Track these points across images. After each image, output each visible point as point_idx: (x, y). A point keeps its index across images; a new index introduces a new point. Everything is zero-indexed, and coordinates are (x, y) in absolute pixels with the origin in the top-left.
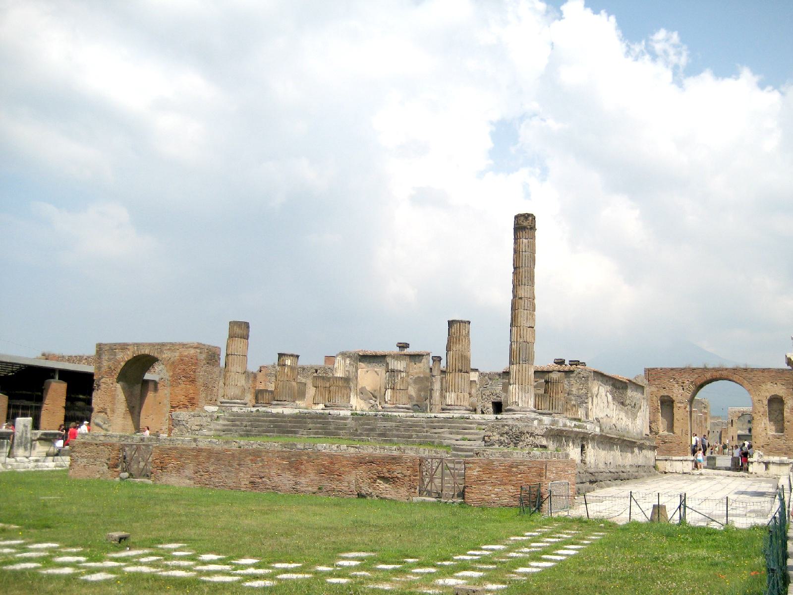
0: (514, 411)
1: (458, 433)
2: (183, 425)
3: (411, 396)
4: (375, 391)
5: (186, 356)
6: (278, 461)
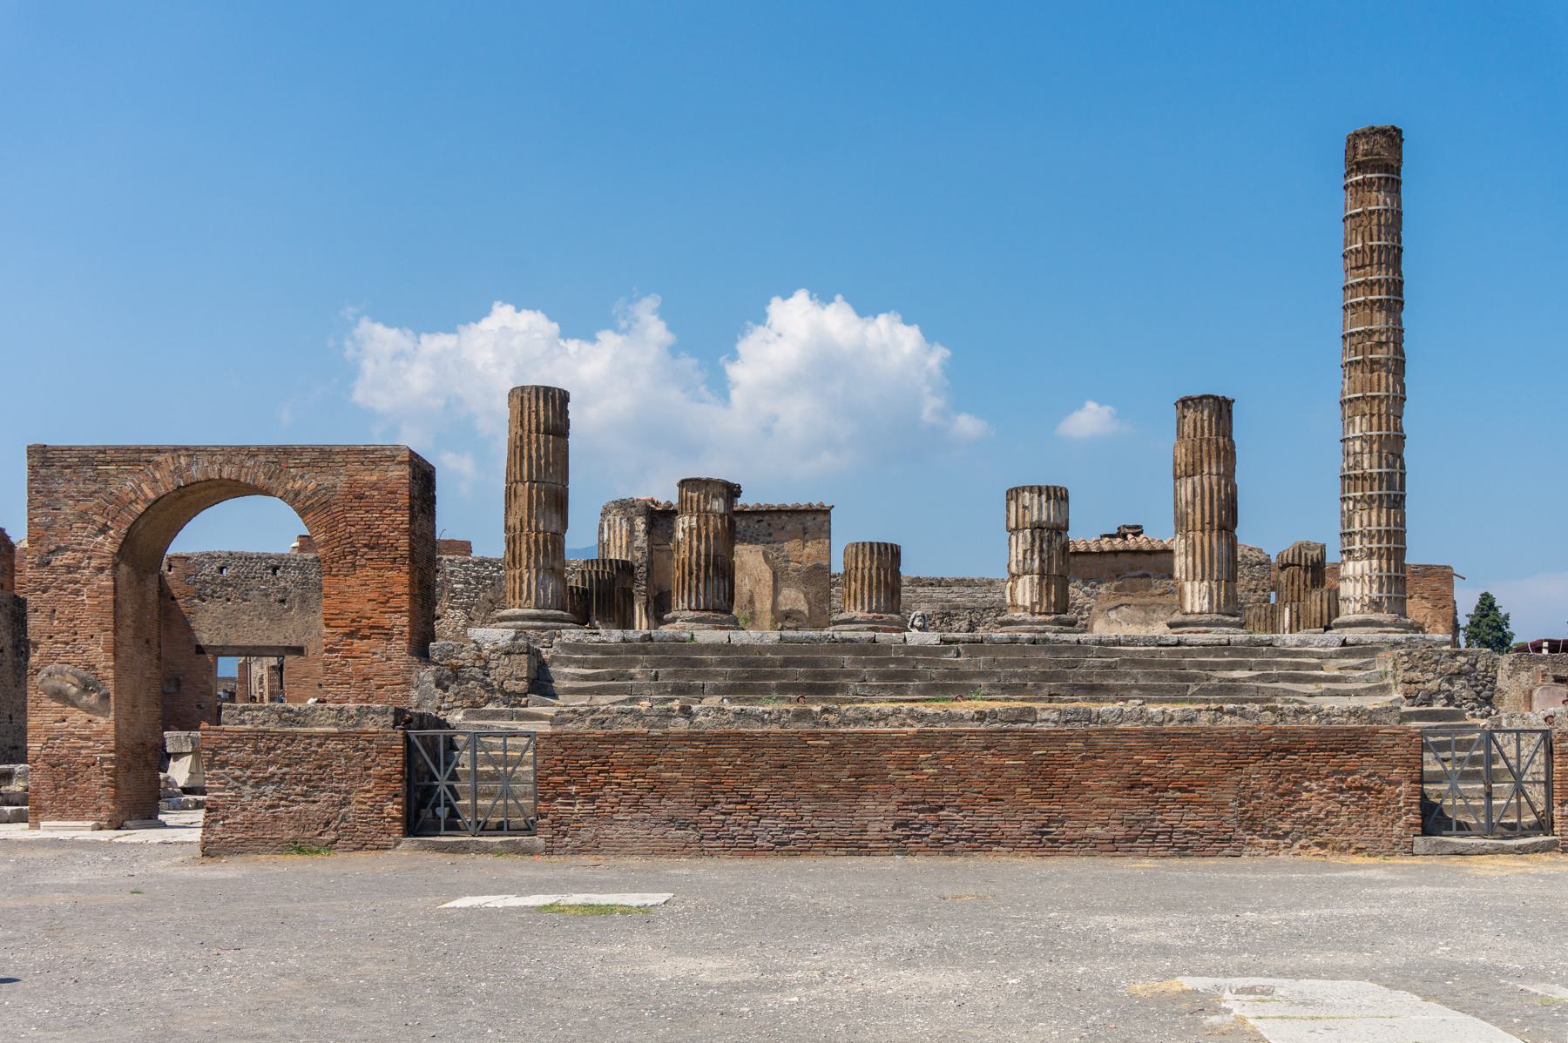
2: (475, 679)
6: (989, 760)
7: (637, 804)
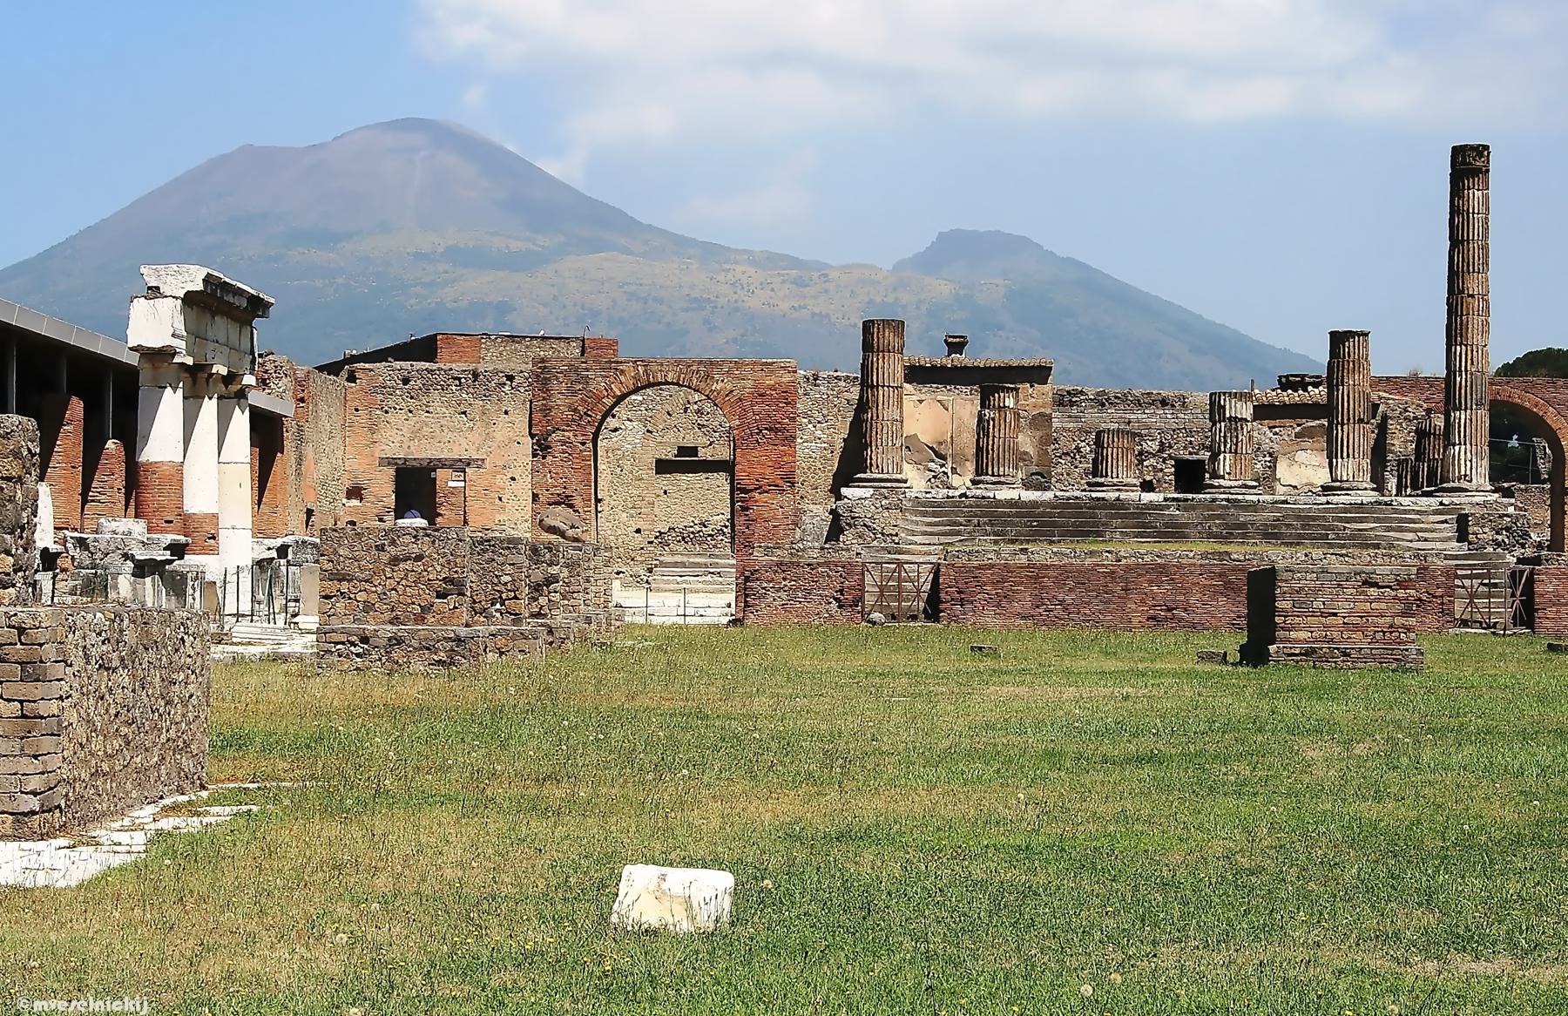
0: (1466, 490)
1: (1401, 530)
3: (1026, 453)
4: (940, 443)
5: (772, 388)
7: (999, 605)
